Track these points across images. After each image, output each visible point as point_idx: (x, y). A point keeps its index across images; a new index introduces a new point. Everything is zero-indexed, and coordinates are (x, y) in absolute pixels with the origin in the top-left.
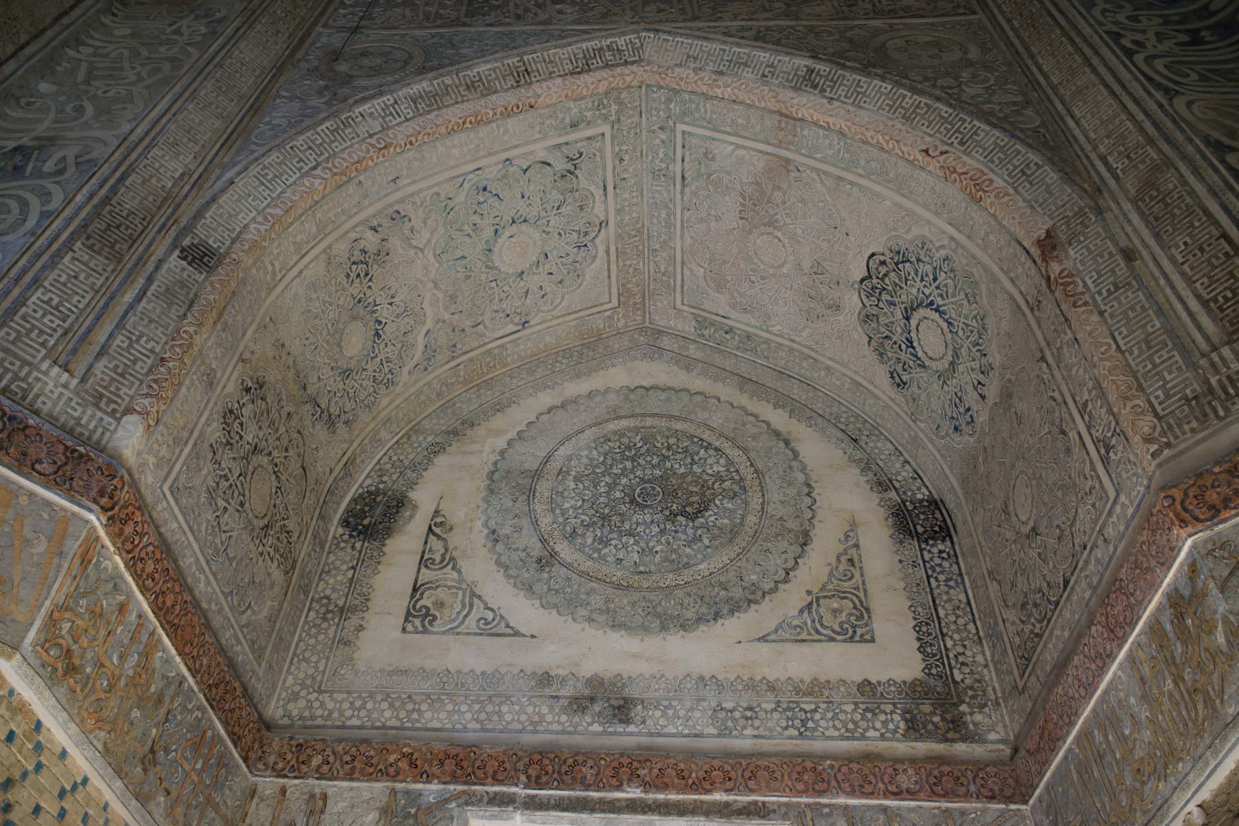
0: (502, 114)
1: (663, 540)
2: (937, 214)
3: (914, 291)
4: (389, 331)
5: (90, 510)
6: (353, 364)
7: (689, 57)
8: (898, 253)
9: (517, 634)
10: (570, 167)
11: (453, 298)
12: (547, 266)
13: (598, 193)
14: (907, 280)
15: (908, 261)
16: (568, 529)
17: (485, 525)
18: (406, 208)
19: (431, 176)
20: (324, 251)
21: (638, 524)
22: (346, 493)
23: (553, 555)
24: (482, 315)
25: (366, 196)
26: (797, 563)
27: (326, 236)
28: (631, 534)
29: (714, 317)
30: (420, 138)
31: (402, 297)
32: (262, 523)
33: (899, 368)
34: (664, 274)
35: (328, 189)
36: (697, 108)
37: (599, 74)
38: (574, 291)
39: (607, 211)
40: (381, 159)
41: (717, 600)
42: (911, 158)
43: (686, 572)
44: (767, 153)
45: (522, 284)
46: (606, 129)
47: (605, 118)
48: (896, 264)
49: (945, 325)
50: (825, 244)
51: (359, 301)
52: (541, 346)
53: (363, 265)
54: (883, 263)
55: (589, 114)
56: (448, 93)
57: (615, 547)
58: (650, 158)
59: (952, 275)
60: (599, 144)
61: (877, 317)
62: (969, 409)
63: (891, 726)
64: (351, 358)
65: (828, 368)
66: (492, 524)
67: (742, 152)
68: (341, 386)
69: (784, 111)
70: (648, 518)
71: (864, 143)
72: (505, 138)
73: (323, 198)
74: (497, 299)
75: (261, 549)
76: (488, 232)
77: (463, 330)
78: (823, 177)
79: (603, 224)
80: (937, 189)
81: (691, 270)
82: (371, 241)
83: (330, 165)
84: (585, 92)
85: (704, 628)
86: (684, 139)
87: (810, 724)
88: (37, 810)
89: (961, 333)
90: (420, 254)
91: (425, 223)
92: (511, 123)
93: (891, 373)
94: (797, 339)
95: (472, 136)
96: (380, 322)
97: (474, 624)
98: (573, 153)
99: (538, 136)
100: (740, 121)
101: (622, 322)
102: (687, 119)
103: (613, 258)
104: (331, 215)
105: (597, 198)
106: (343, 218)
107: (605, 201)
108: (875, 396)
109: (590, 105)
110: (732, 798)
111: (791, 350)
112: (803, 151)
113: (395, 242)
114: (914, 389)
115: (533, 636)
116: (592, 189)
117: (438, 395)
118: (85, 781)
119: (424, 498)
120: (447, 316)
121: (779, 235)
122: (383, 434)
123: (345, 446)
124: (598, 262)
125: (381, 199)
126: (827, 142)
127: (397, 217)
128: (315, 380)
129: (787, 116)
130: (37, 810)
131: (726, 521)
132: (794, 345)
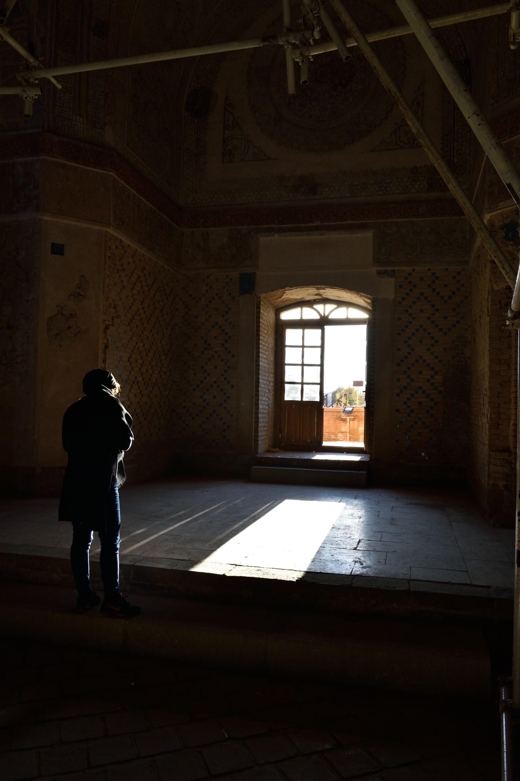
5: (110, 171)
63: (422, 187)
87: (388, 189)
88: (129, 263)
110: (353, 222)
118: (136, 250)
130: (129, 263)
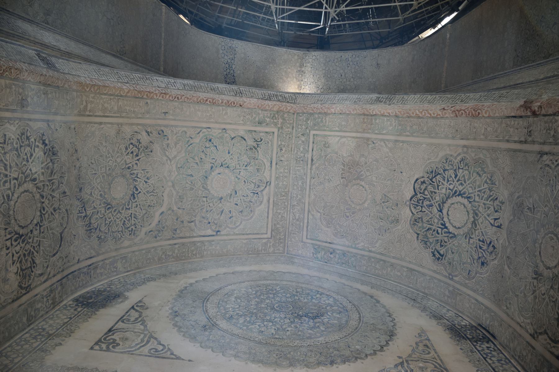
0: (226, 103)
1: (292, 326)
2: (453, 138)
3: (444, 191)
4: (141, 197)
6: (114, 203)
7: (318, 100)
8: (432, 172)
9: (178, 358)
10: (255, 144)
11: (181, 198)
12: (235, 199)
13: (268, 164)
14: (438, 186)
15: (439, 174)
16: (227, 315)
17: (172, 309)
18: (167, 131)
19: (185, 121)
20: (118, 124)
21: (275, 318)
22: (84, 286)
23: (215, 325)
24: (195, 216)
25: (148, 112)
26: (387, 343)
27: (121, 117)
28: (270, 321)
29: (324, 244)
30: (183, 98)
31: (153, 182)
32: (17, 228)
33: (438, 247)
34: (298, 220)
35: (129, 94)
36: (322, 121)
37: (275, 103)
38: (248, 220)
39: (271, 177)
40: (161, 98)
41: (333, 355)
42: (435, 115)
43: (309, 340)
44: (357, 138)
45: (220, 205)
46: (276, 130)
47: (276, 124)
48: (431, 180)
49: (465, 201)
50: (389, 182)
51: (129, 168)
52: (225, 251)
53: (137, 149)
54: (424, 182)
55: (268, 120)
56: (201, 88)
57: (259, 325)
58: (296, 151)
59: (467, 168)
60: (271, 137)
61: (421, 218)
62: (490, 243)
64: (114, 199)
65: (392, 265)
66: (176, 309)
67: (344, 140)
68: (103, 210)
69: (366, 113)
70: (282, 316)
71: (409, 117)
72: (225, 117)
73: (126, 96)
74: (205, 210)
75: (8, 243)
76: (208, 166)
77: (182, 222)
78: (387, 143)
79: (268, 183)
80: (452, 124)
81: (313, 215)
82: (144, 138)
83: (134, 86)
84: (267, 108)
85: (323, 368)
86: (314, 138)
89: (477, 199)
90: (169, 161)
91: (175, 145)
92: (229, 110)
93: (433, 253)
94: (373, 249)
95: (209, 109)
96: (137, 190)
97: (147, 351)
98: (257, 138)
99: (242, 122)
100: (343, 123)
101: (272, 249)
102: (316, 128)
103: (271, 206)
104: (128, 108)
105: (267, 167)
106: (133, 115)
107: (271, 170)
108: (424, 274)
109: (269, 115)
111: (370, 258)
112: (376, 132)
113: (156, 147)
114: (450, 256)
115: (190, 361)
116: (265, 161)
117: (160, 259)
119: (134, 296)
120: (175, 208)
121: (363, 183)
122: (119, 265)
123: (94, 254)
124: (263, 206)
125: (155, 119)
126: (389, 123)
127: (161, 133)
128: (89, 192)
129: (367, 115)
131: (336, 322)
132: (372, 255)
